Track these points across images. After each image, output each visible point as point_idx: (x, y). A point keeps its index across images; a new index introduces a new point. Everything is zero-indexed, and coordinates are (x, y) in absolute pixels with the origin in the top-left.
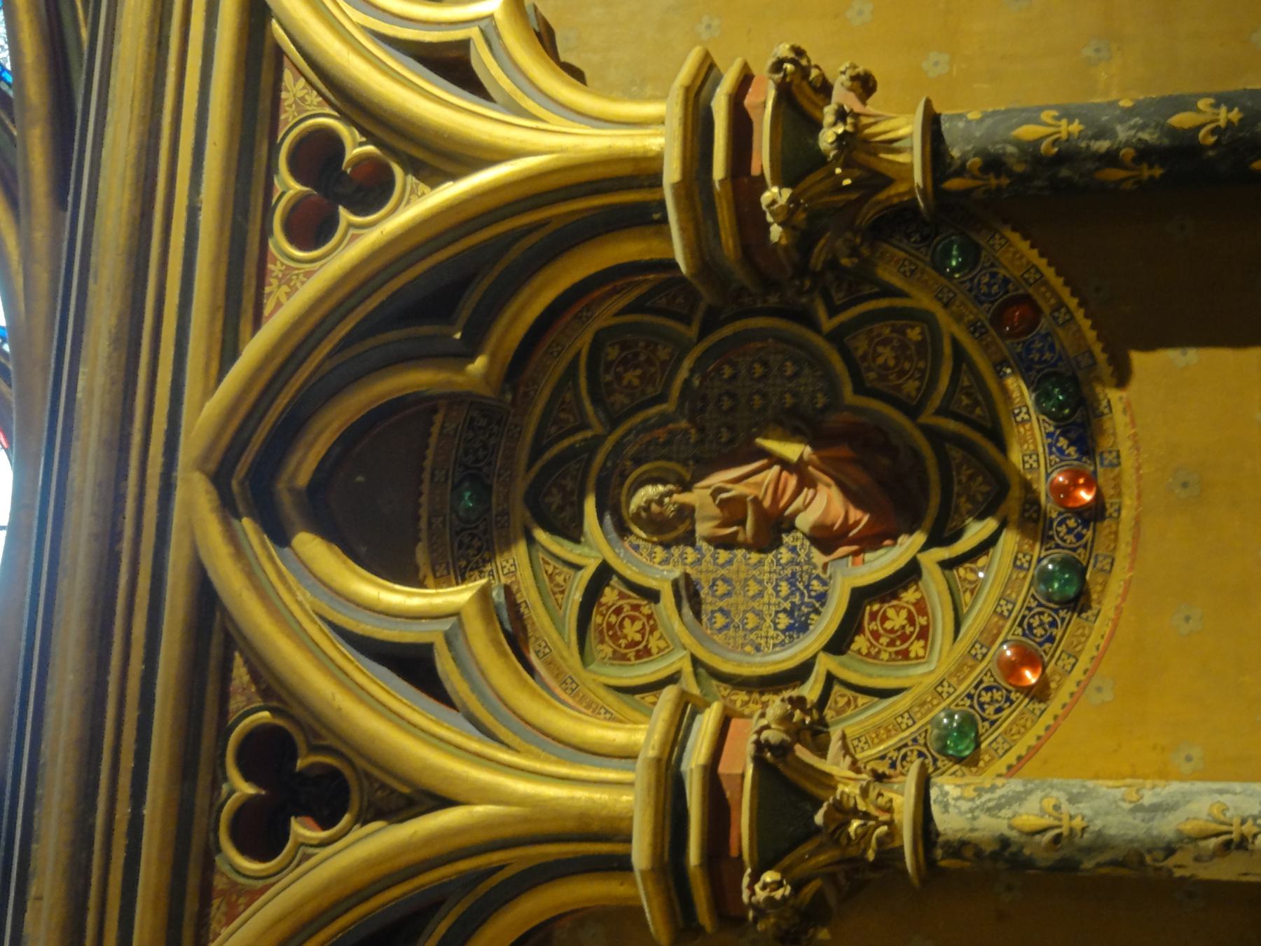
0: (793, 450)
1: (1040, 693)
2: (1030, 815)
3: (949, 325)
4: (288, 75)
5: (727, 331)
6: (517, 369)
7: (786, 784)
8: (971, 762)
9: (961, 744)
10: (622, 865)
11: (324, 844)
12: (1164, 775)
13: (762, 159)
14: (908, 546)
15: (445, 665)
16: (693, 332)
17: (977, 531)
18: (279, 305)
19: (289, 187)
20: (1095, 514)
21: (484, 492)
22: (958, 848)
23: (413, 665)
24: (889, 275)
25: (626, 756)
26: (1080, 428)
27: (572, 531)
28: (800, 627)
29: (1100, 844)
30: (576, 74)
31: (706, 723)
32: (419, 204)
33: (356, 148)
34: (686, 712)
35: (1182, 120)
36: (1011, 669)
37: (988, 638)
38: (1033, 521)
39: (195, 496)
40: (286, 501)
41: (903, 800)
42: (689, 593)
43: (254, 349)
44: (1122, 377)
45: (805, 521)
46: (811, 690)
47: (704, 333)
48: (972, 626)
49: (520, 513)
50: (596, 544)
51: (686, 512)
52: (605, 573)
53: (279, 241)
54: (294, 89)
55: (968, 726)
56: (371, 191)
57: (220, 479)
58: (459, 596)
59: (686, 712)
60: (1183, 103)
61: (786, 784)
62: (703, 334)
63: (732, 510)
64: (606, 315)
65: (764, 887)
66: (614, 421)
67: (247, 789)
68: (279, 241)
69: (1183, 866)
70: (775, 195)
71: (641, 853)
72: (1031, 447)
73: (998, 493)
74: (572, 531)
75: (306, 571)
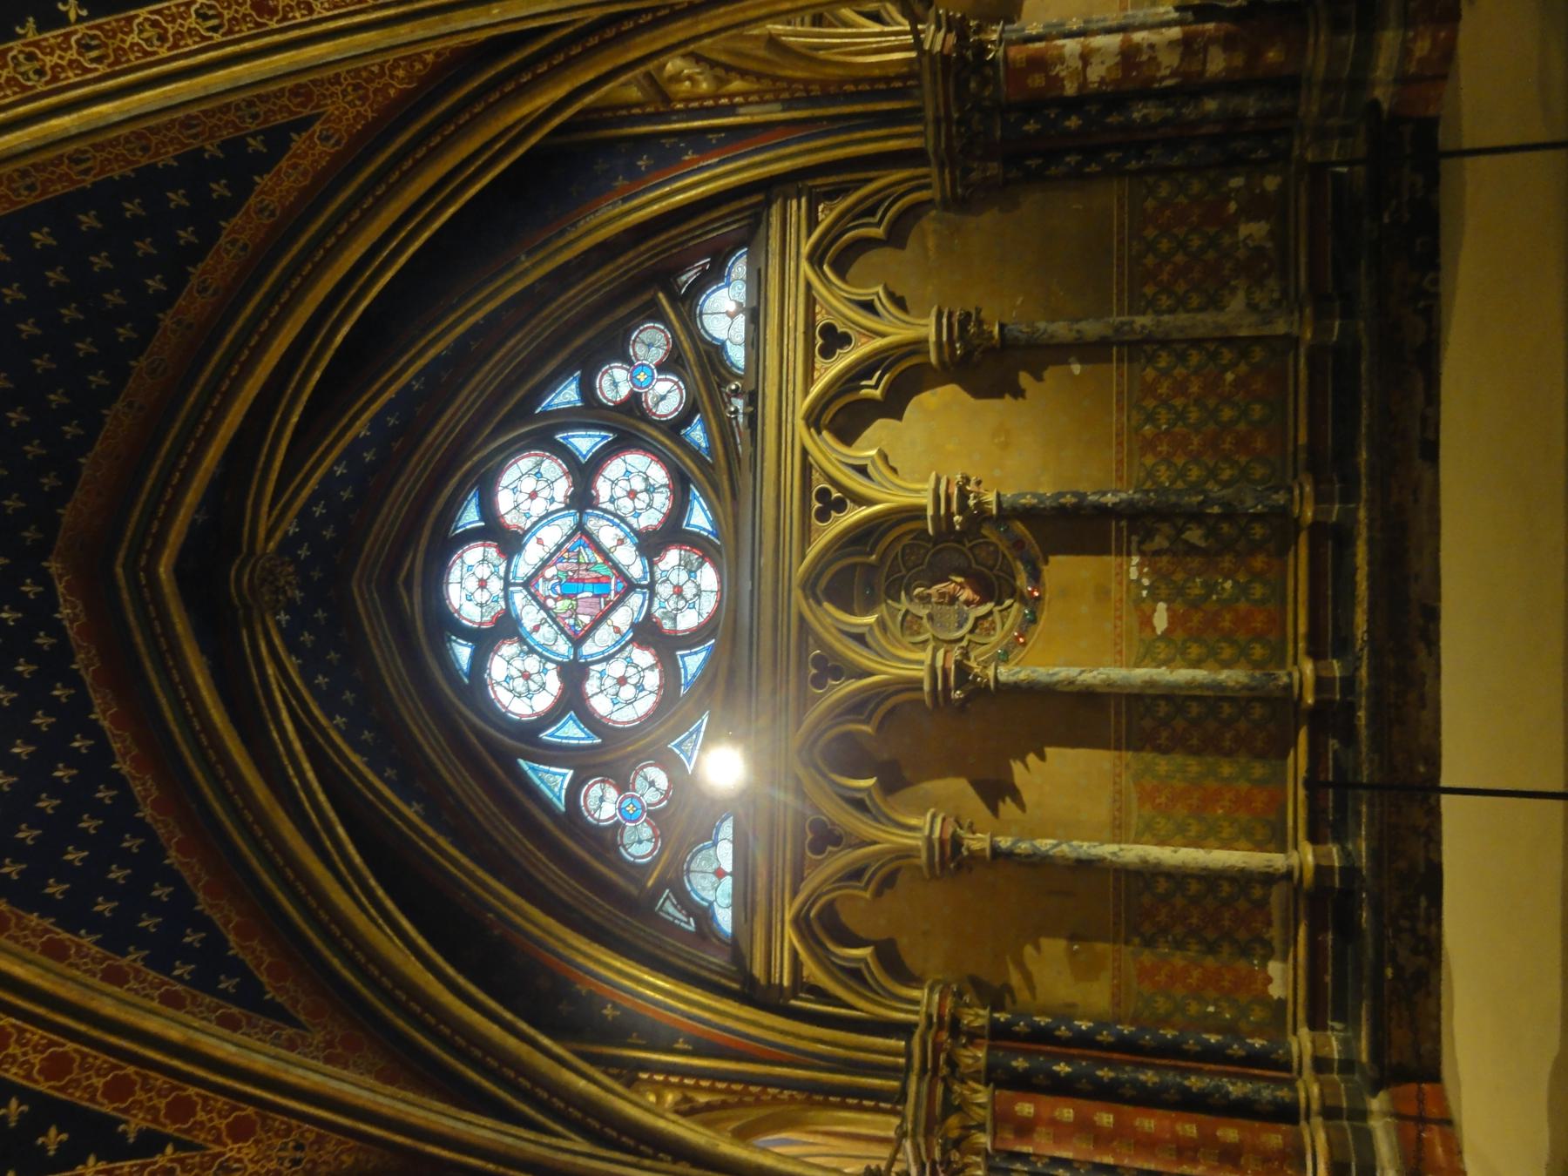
0: (959, 580)
1: (1024, 644)
2: (1022, 676)
3: (1002, 548)
6: (882, 559)
7: (962, 669)
8: (1006, 661)
9: (1004, 658)
10: (921, 689)
12: (1055, 665)
13: (954, 507)
14: (989, 606)
15: (869, 639)
17: (1008, 602)
19: (817, 505)
20: (1038, 599)
21: (872, 589)
22: (1005, 684)
23: (860, 639)
24: (985, 532)
25: (921, 662)
26: (1035, 577)
27: (898, 600)
28: (960, 626)
29: (1039, 683)
30: (894, 470)
32: (855, 515)
33: (836, 494)
34: (935, 650)
35: (1062, 500)
36: (1017, 638)
37: (1011, 630)
38: (1023, 599)
39: (797, 593)
40: (819, 592)
41: (991, 672)
42: (930, 617)
43: (812, 552)
44: (1046, 562)
45: (963, 598)
46: (964, 643)
48: (1007, 626)
49: (883, 596)
50: (904, 604)
51: (929, 595)
52: (907, 612)
53: (814, 520)
54: (816, 475)
55: (1006, 653)
56: (840, 506)
57: (803, 588)
58: (871, 619)
59: (935, 650)
60: (1062, 494)
61: (962, 669)
63: (942, 595)
64: (906, 540)
65: (957, 695)
66: (909, 570)
67: (814, 671)
68: (814, 520)
69: (1059, 688)
70: (957, 518)
71: (926, 687)
72: (1022, 581)
73: (1014, 593)
74: (898, 600)
75: (826, 611)
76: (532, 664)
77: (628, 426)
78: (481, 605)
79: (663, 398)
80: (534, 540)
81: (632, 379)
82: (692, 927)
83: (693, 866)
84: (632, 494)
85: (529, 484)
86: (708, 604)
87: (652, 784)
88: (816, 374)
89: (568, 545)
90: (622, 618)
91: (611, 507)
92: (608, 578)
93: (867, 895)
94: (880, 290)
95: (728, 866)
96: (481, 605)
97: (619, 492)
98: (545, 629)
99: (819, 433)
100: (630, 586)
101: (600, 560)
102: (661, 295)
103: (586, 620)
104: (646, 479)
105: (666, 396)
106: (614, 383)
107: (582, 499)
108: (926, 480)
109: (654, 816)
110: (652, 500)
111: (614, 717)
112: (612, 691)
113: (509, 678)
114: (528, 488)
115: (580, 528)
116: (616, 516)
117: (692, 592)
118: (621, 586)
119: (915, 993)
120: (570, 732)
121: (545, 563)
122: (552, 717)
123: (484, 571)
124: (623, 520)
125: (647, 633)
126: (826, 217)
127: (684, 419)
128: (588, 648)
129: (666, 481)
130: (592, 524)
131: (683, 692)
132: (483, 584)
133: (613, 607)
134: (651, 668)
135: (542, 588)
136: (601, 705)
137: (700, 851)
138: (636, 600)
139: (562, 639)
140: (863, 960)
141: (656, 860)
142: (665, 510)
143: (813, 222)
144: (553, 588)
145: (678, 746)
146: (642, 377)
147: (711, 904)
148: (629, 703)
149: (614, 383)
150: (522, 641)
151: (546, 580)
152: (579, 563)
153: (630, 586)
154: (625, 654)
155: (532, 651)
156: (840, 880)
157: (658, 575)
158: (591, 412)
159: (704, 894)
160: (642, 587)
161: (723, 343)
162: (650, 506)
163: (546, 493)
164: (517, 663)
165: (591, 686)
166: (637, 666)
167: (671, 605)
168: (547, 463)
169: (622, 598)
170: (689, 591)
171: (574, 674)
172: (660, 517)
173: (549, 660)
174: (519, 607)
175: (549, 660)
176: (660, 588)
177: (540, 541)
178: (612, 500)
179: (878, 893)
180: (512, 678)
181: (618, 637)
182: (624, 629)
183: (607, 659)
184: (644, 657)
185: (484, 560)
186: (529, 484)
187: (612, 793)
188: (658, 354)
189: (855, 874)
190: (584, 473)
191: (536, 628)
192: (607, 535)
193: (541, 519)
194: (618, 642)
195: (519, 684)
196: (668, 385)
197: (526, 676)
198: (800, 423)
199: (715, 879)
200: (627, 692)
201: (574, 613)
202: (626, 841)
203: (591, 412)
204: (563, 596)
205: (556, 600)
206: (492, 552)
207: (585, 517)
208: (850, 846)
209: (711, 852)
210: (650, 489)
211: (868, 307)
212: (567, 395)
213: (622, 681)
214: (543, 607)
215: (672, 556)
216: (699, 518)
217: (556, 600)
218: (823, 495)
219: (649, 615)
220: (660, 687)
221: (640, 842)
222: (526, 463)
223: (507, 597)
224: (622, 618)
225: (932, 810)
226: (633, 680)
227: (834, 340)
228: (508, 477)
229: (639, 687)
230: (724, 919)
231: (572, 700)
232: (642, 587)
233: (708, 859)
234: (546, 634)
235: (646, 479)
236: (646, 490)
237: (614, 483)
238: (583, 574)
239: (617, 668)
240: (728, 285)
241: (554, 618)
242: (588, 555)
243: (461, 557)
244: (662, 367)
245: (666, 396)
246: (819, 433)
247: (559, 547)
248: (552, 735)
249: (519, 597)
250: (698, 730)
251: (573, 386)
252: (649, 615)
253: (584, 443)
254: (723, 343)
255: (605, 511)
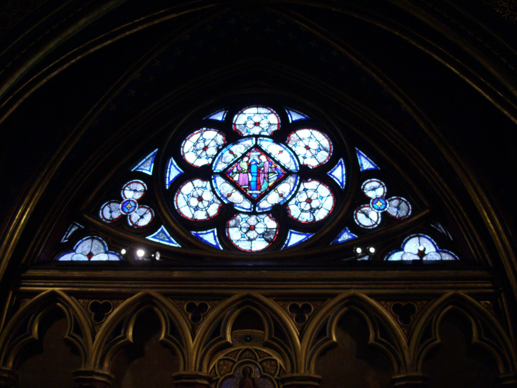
4: (321, 302)
5: (276, 383)
11: (188, 319)
16: (276, 377)
18: (279, 304)
25: (201, 370)
30: (323, 353)
31: (206, 382)
43: (270, 302)
47: (276, 379)
62: (276, 379)
76: (212, 151)
77: (349, 198)
78: (245, 124)
79: (367, 216)
80: (282, 149)
81: (378, 199)
82: (64, 241)
83: (95, 241)
84: (309, 201)
85: (314, 145)
86: (244, 246)
87: (142, 217)
88: (382, 302)
89: (279, 167)
90: (237, 197)
91: (301, 189)
92: (260, 190)
93: (66, 336)
94: (438, 341)
95: (93, 259)
96: (245, 124)
97: (310, 193)
98: (231, 157)
99: (346, 305)
100: (255, 202)
101: (270, 184)
102: (428, 211)
103: (236, 178)
104: (318, 208)
105: (368, 218)
106: (374, 189)
107: (305, 173)
108: (317, 371)
109: (123, 219)
110: (306, 211)
111: (180, 195)
112: (195, 194)
113: (205, 140)
114: (311, 145)
115: (288, 173)
116: (296, 192)
117: (251, 236)
118: (255, 196)
119: (10, 364)
120: (173, 172)
121: (268, 155)
122: (182, 162)
123: (264, 124)
124: (294, 196)
125: (228, 211)
126: (482, 305)
127: (356, 228)
128: (219, 180)
129: (317, 219)
130: (291, 179)
131: (193, 232)
132: (257, 124)
133: (243, 192)
134: (207, 214)
135: (254, 155)
136: (187, 188)
137: (103, 244)
138: (247, 205)
139: (225, 166)
140: (31, 333)
141: (100, 220)
142: (300, 219)
143: (479, 297)
144: (254, 160)
145: (162, 231)
146: (379, 204)
147: (74, 251)
148: (188, 203)
149: (374, 189)
150: (225, 146)
151: (259, 156)
152: (268, 173)
153: (255, 202)
154: (216, 200)
155: (219, 150)
156: (75, 320)
157: (262, 216)
158: (356, 177)
159: (80, 247)
160: (254, 208)
161: (402, 250)
162: (302, 211)
163: (308, 154)
164: (213, 143)
165: (198, 182)
166: (208, 206)
167: (243, 224)
168: (327, 154)
169: (248, 197)
170: (252, 234)
171: (206, 173)
172: (296, 217)
173: (214, 159)
174: (244, 143)
175: (214, 159)
176: (253, 218)
177: (281, 152)
178: (305, 190)
179: (68, 343)
180: (204, 142)
181: (226, 196)
182: (230, 199)
183: (213, 190)
184: (213, 210)
185: (270, 124)
186: (314, 145)
187: (138, 196)
188: (393, 211)
189: (78, 329)
190: (321, 173)
191: (231, 152)
192: (285, 188)
193: (294, 152)
194: (222, 196)
195: (201, 145)
196: (375, 218)
197: (205, 148)
198: (352, 292)
199: (87, 253)
200: (194, 202)
201: (239, 172)
202: (112, 204)
203: (356, 177)
204: (250, 166)
205: (247, 162)
206: (275, 128)
207: (295, 175)
208: (93, 326)
209: (102, 251)
210: (312, 210)
211: (427, 334)
212: (366, 164)
213: (200, 199)
214: (244, 155)
215: (272, 224)
216: (295, 238)
217: (247, 162)
218: (307, 308)
219: (238, 212)
220: (196, 220)
221: (111, 212)
222: (325, 142)
223: (250, 137)
224: (237, 197)
225: (113, 376)
226: (200, 205)
227: (404, 313)
228: (318, 135)
229: (196, 208)
230: (66, 258)
231: (190, 173)
232: (254, 208)
233: (98, 249)
234: (228, 158)
235: (318, 208)
236: (311, 209)
237: (316, 191)
238: (262, 176)
239: (208, 196)
240: (437, 251)
241: (237, 162)
242: (273, 178)
243: (272, 112)
244: (385, 215)
245: (368, 218)
246: (346, 305)
247: (278, 163)
248: (172, 163)
249: (250, 143)
250: (171, 241)
251: (372, 167)
252: (238, 212)
253: (338, 173)
254: (402, 250)
255: (299, 186)
